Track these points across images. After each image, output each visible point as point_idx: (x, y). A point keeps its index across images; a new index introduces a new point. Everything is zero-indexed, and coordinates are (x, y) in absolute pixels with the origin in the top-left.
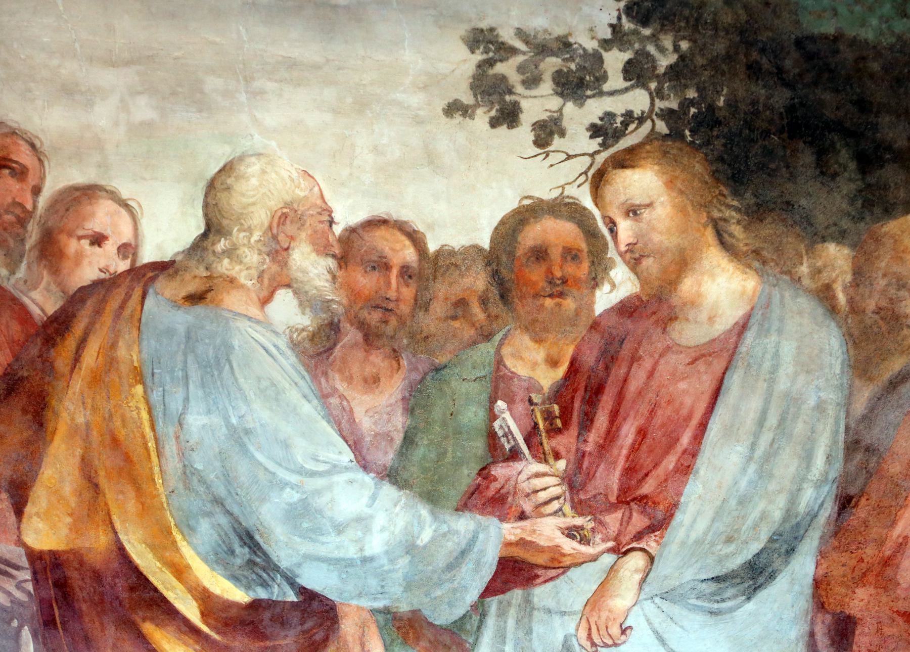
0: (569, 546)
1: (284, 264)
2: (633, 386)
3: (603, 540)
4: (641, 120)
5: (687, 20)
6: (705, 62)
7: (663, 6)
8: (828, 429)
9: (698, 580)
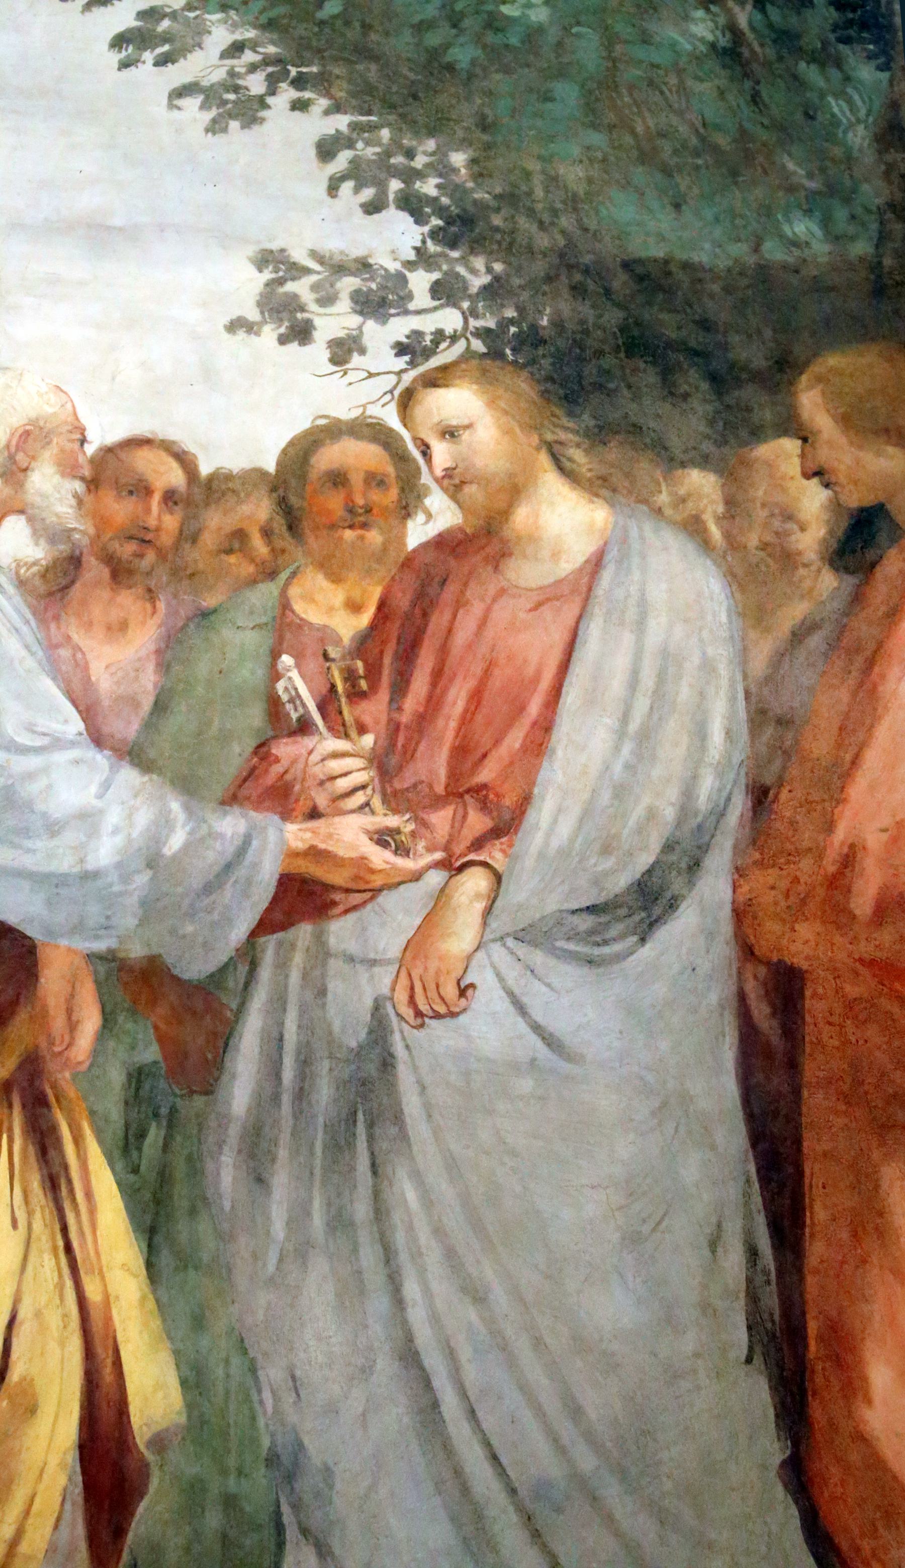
0: (380, 857)
1: (19, 485)
2: (461, 637)
3: (430, 849)
4: (454, 338)
5: (499, 243)
6: (523, 282)
7: (472, 231)
8: (722, 693)
9: (568, 911)
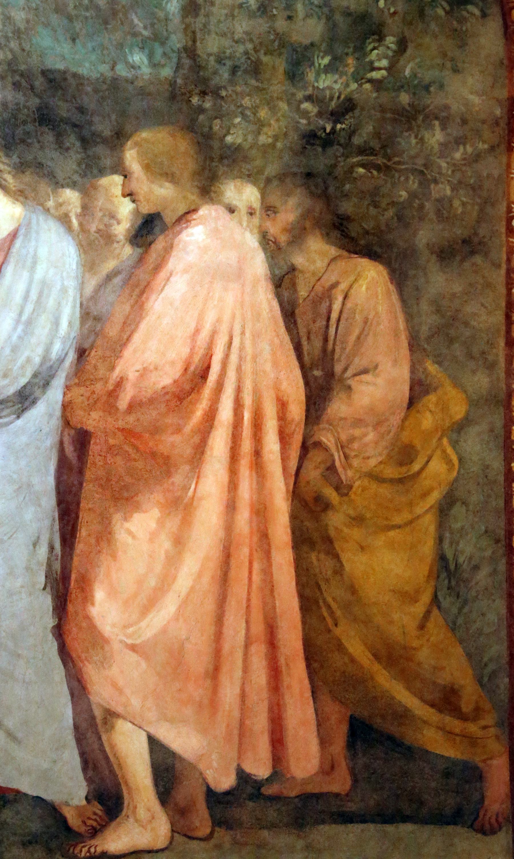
8: (70, 304)
